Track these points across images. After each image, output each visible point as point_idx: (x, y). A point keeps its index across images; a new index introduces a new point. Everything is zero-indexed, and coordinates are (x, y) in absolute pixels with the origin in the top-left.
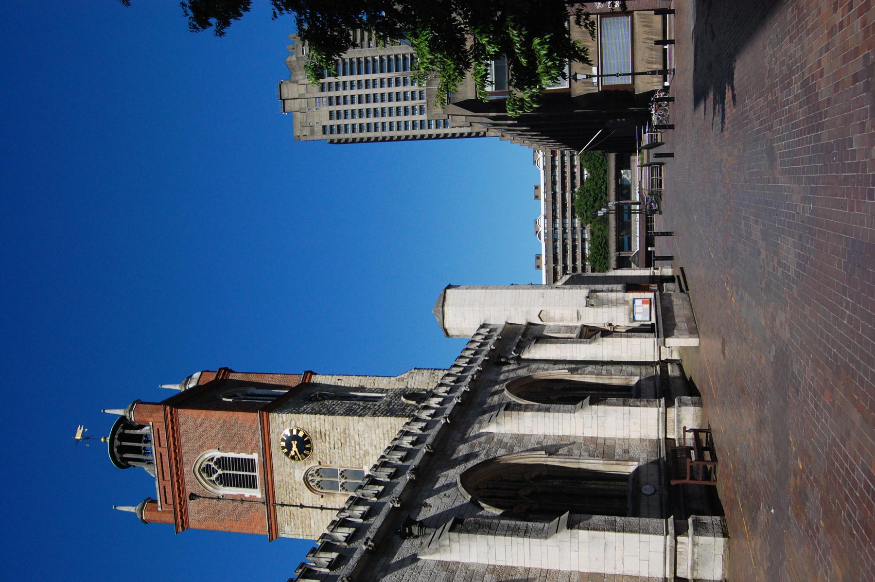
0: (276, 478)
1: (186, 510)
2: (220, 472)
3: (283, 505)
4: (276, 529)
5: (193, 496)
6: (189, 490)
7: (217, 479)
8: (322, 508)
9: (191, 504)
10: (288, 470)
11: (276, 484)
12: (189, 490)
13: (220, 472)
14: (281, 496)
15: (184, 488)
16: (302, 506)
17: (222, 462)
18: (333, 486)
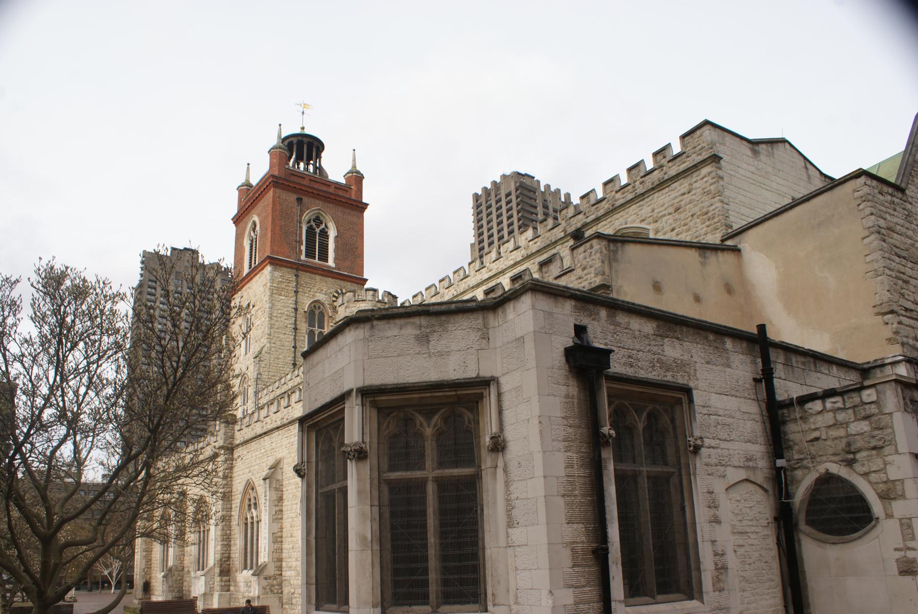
0: (318, 277)
1: (288, 190)
2: (318, 231)
3: (297, 276)
4: (277, 265)
5: (299, 200)
6: (305, 200)
7: (311, 226)
8: (296, 309)
9: (295, 196)
10: (325, 289)
11: (313, 276)
12: (305, 200)
13: (318, 231)
14: (305, 277)
15: (305, 195)
16: (296, 292)
17: (324, 234)
18: (311, 324)
